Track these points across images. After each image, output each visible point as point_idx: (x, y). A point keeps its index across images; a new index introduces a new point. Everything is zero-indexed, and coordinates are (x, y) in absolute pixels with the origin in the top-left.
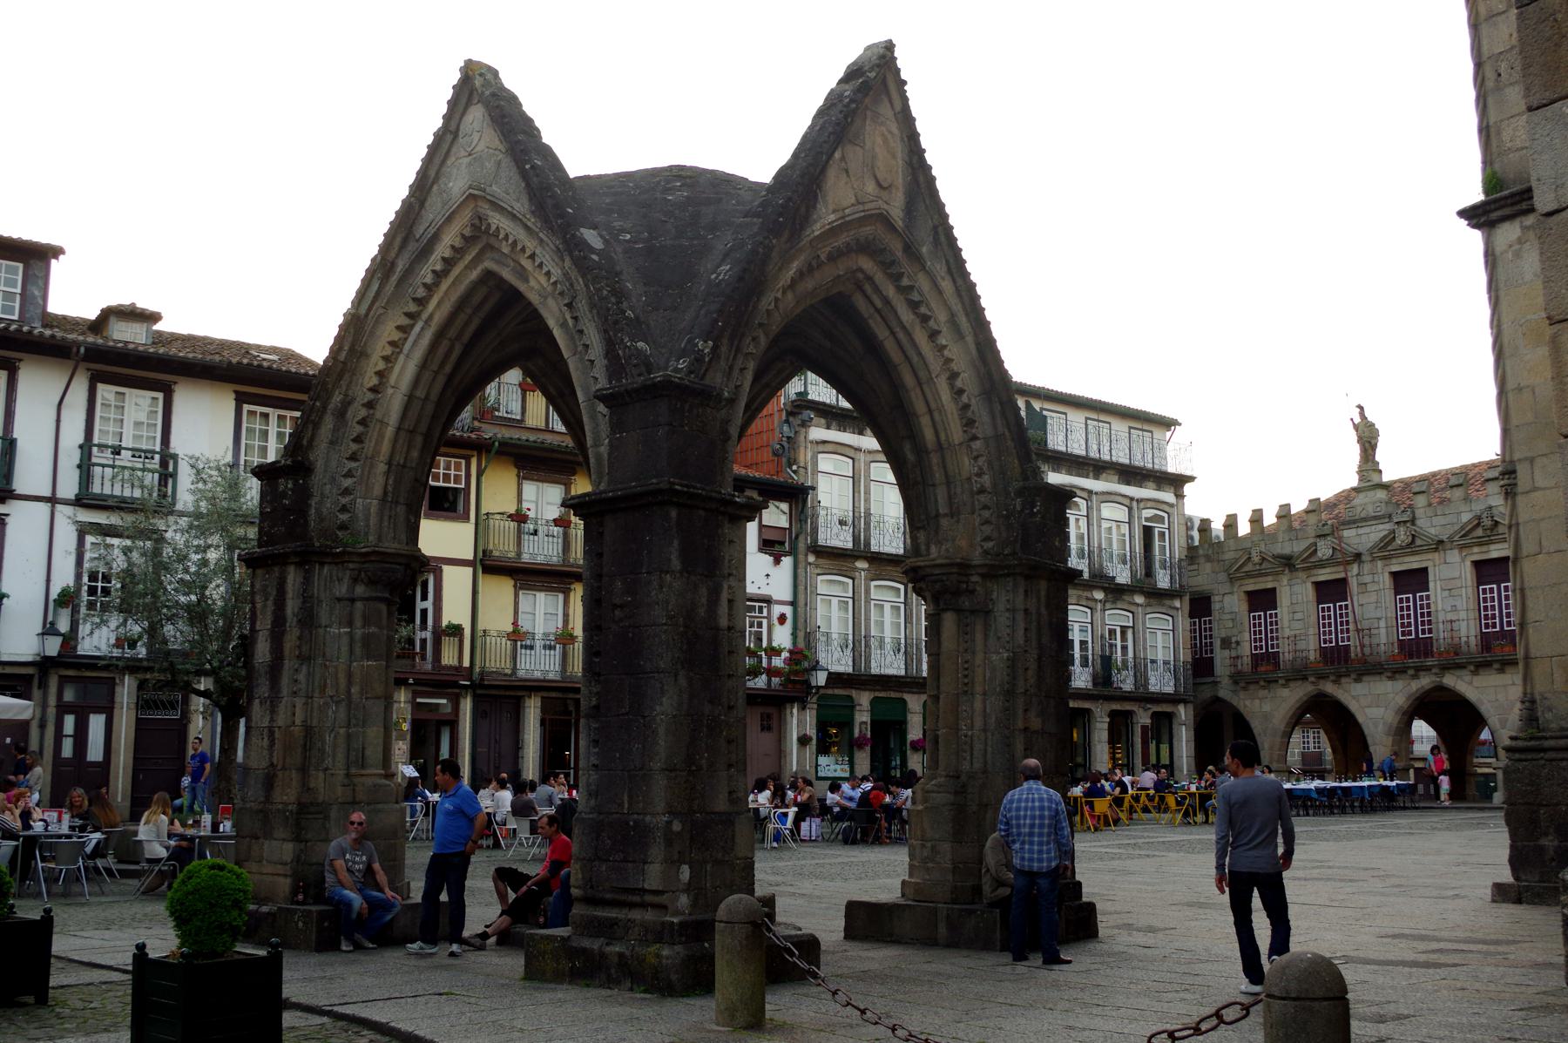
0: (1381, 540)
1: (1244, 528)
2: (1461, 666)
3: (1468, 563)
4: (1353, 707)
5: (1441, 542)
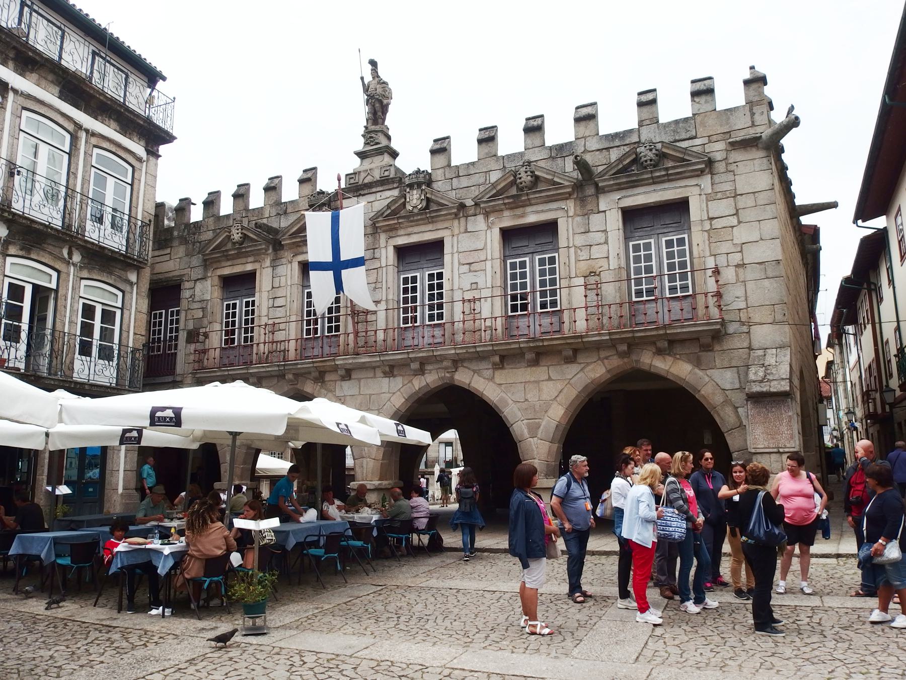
0: (388, 207)
1: (226, 207)
2: (481, 357)
3: (496, 232)
5: (462, 206)
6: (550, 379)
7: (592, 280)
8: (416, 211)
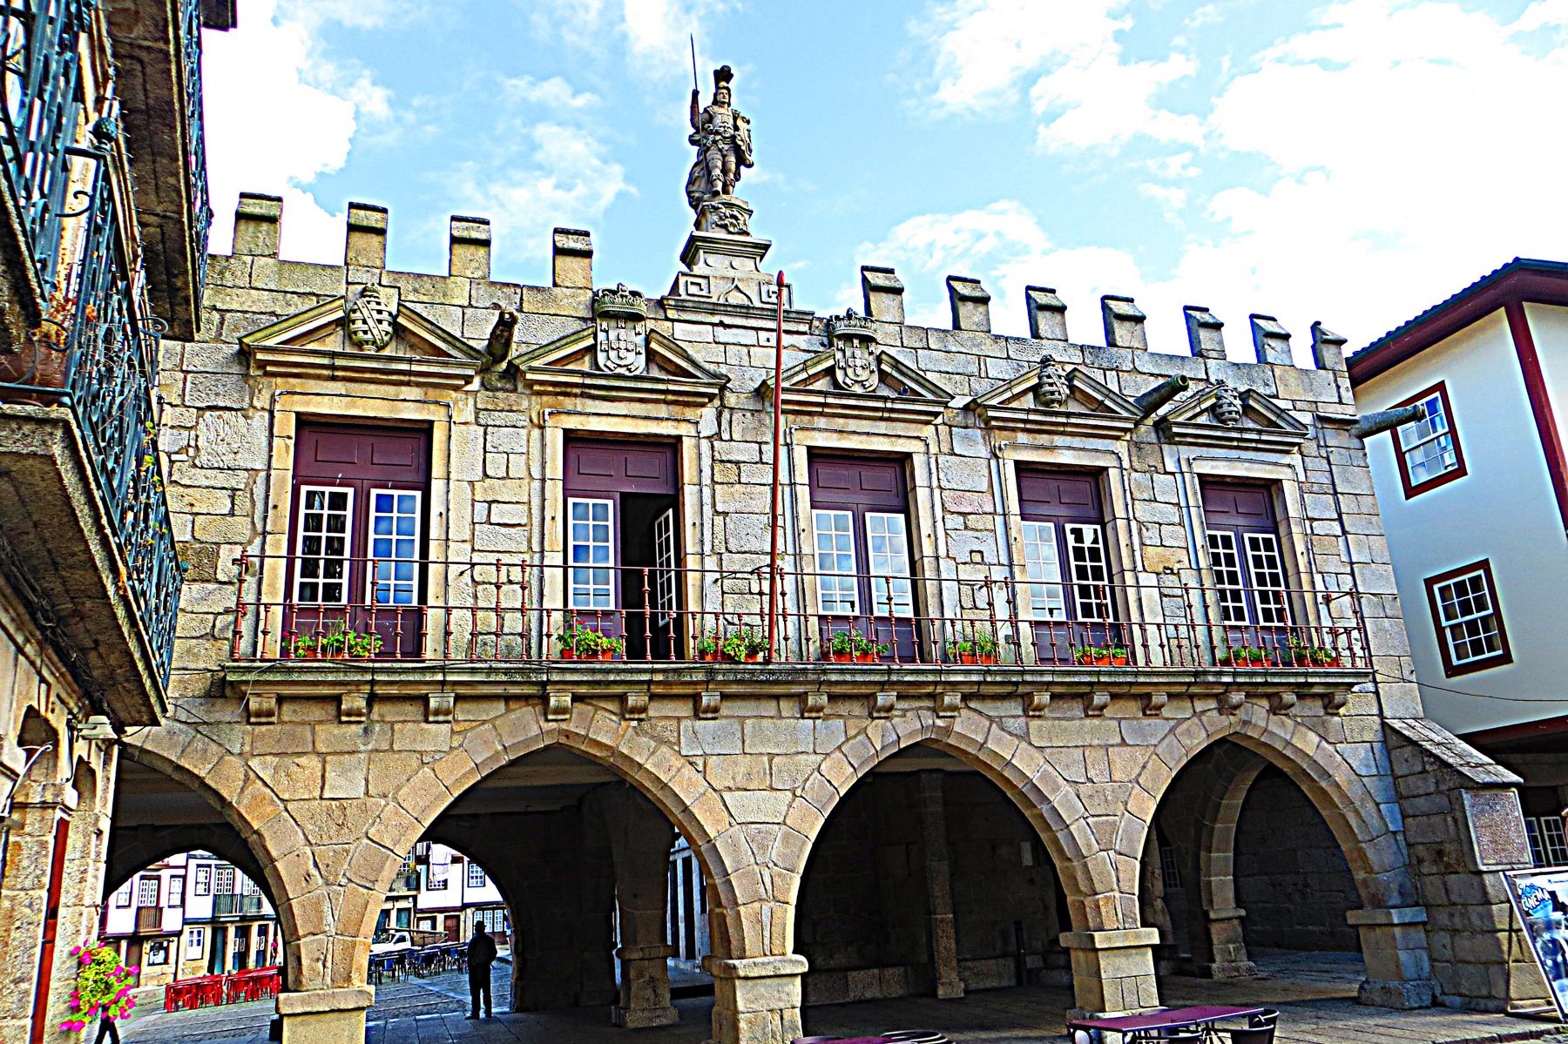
4: (686, 786)
6: (1124, 743)
7: (1170, 580)
8: (858, 389)
